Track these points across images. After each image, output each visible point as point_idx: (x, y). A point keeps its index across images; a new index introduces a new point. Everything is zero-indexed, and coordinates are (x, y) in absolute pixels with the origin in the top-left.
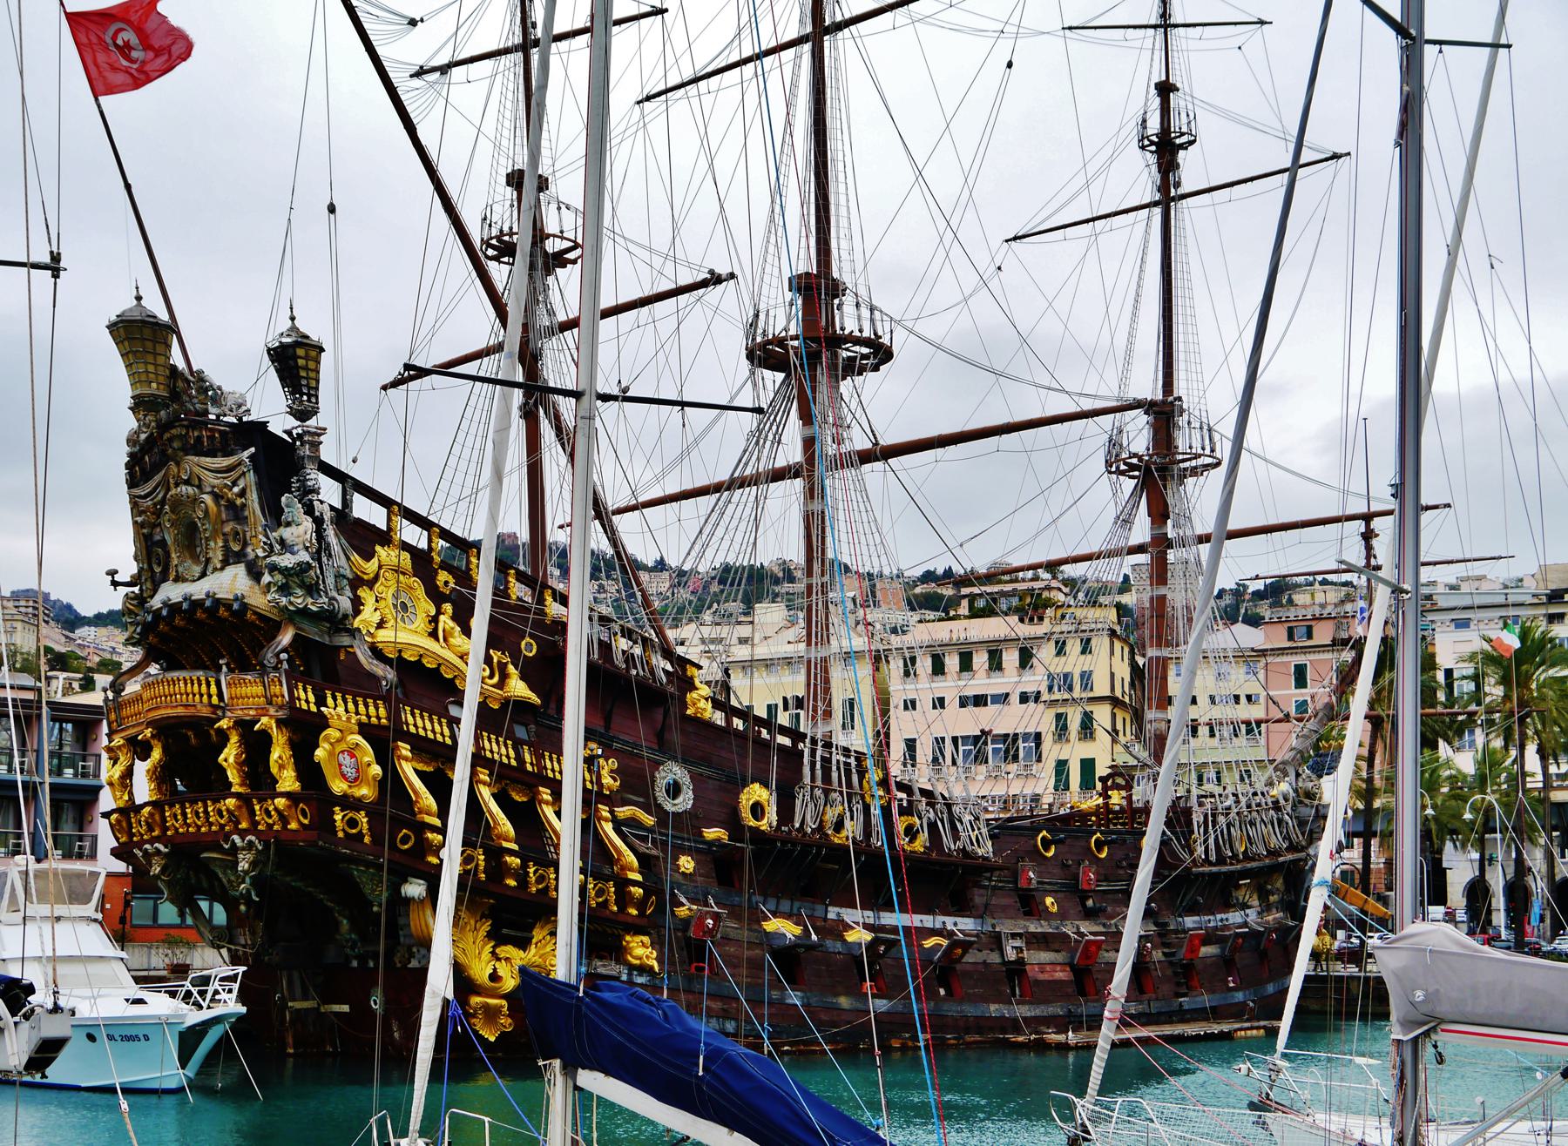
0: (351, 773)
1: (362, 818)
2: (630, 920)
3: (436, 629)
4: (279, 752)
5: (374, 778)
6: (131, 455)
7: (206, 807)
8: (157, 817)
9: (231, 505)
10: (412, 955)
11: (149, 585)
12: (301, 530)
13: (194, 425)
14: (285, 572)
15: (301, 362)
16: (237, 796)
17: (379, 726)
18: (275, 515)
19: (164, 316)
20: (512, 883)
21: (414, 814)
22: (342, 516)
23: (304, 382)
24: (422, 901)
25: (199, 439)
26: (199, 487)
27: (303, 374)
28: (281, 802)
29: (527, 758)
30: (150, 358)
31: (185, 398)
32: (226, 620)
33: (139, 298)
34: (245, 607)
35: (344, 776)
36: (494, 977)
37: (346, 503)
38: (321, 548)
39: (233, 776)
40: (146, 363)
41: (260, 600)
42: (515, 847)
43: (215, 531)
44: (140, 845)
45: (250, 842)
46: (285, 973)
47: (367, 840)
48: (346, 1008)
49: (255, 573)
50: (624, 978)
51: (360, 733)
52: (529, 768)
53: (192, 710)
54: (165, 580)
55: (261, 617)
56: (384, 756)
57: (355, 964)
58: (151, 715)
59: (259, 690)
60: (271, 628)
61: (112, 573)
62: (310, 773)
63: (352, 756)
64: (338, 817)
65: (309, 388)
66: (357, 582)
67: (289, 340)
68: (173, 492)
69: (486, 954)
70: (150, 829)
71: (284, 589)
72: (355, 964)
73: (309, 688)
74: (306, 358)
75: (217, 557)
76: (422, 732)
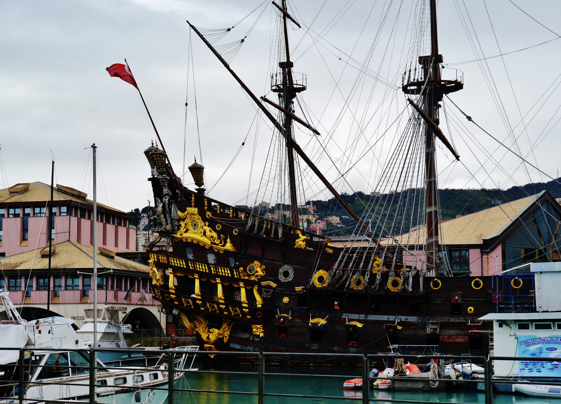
15: (155, 159)
36: (208, 338)
50: (251, 339)
66: (180, 219)
69: (206, 331)
74: (157, 157)
76: (176, 265)
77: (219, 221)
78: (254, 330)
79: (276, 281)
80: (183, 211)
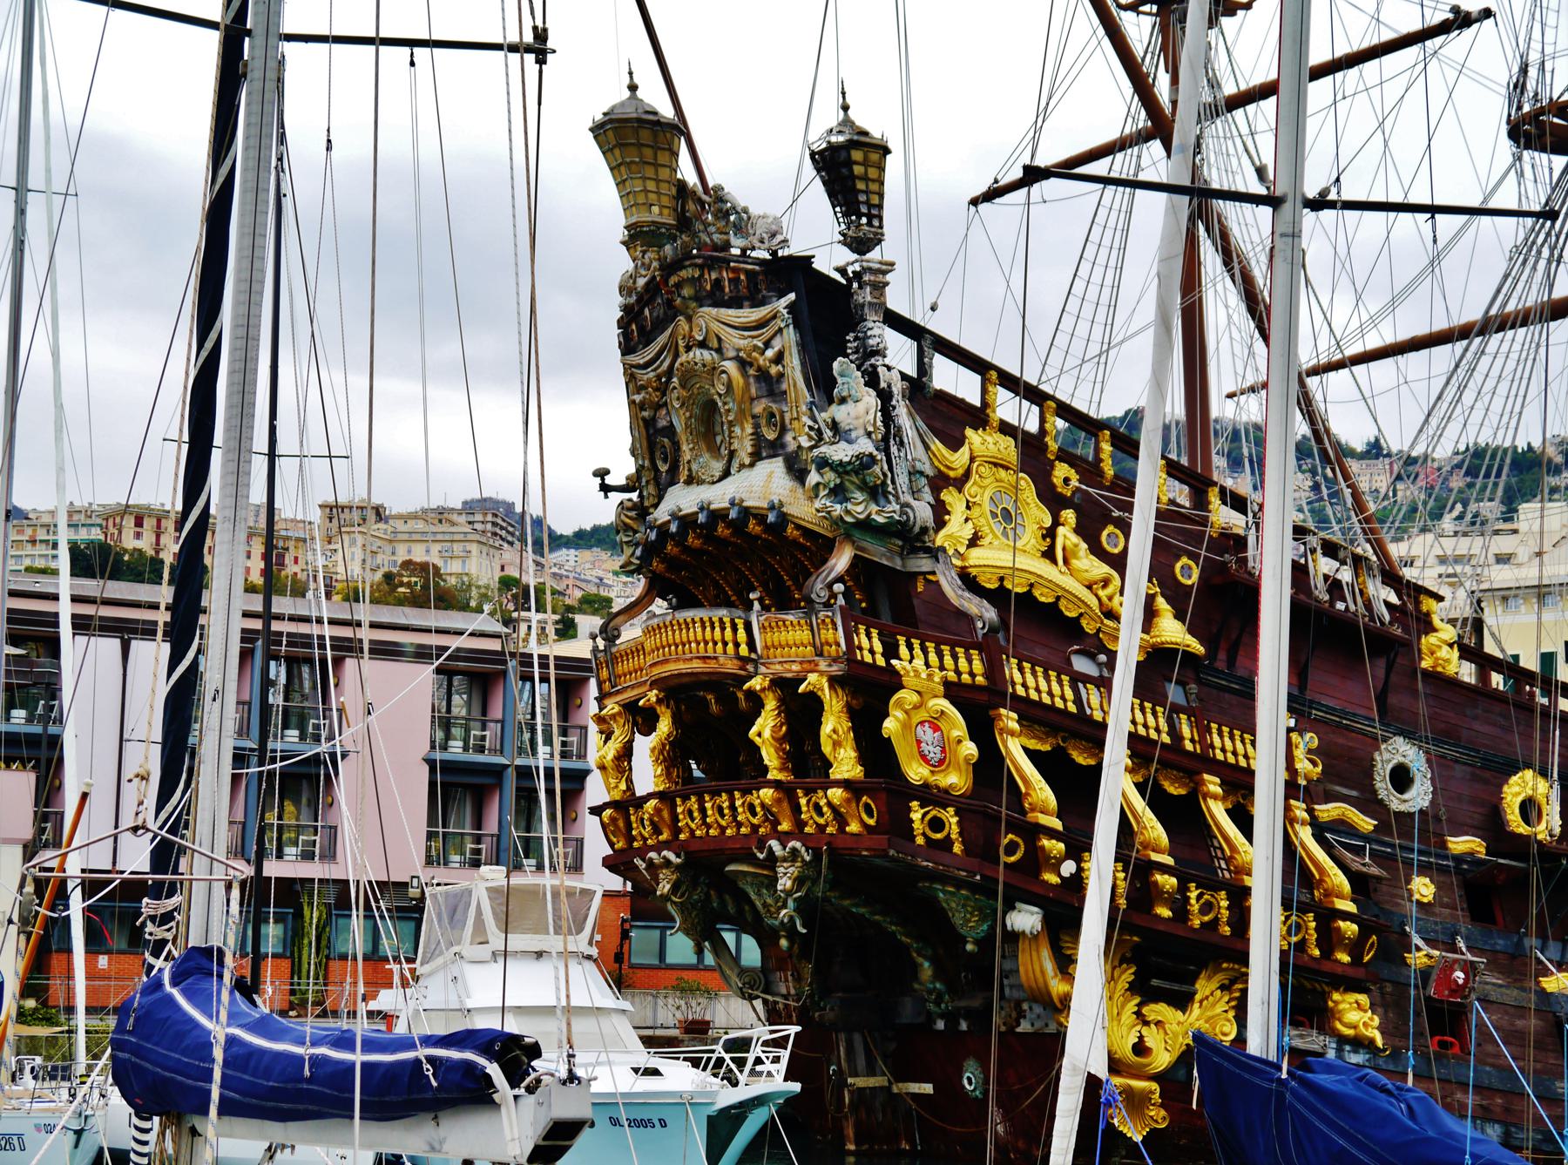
0: (934, 753)
1: (951, 818)
2: (1339, 970)
3: (1052, 547)
4: (834, 722)
5: (967, 760)
6: (626, 309)
7: (732, 800)
8: (665, 814)
9: (763, 376)
10: (1021, 1015)
11: (652, 489)
12: (860, 409)
13: (710, 264)
14: (840, 468)
15: (858, 170)
16: (777, 785)
17: (973, 687)
18: (824, 386)
19: (667, 111)
20: (1164, 912)
21: (1024, 812)
22: (918, 387)
23: (862, 198)
24: (1035, 937)
25: (718, 283)
26: (719, 350)
27: (861, 186)
28: (836, 794)
29: (1186, 731)
30: (650, 172)
31: (699, 226)
32: (757, 537)
33: (633, 88)
34: (784, 518)
35: (924, 757)
36: (1140, 1048)
37: (923, 368)
38: (889, 435)
39: (770, 757)
40: (644, 179)
41: (805, 509)
42: (1170, 861)
43: (741, 413)
44: (642, 853)
45: (794, 850)
46: (842, 1036)
47: (957, 848)
48: (928, 1088)
49: (797, 472)
50: (1331, 1054)
51: (946, 696)
52: (1189, 746)
53: (713, 664)
54: (673, 483)
55: (807, 532)
56: (982, 730)
57: (940, 1025)
58: (656, 671)
59: (805, 635)
60: (821, 547)
61: (602, 473)
62: (877, 753)
63: (936, 728)
64: (916, 816)
65: (870, 206)
66: (940, 482)
67: (841, 139)
68: (683, 358)
70: (657, 831)
71: (838, 493)
72: (940, 1025)
73: (874, 632)
74: (866, 163)
75: (744, 448)
77: (1116, 513)
78: (1353, 1016)
79: (1370, 803)
80: (955, 443)
